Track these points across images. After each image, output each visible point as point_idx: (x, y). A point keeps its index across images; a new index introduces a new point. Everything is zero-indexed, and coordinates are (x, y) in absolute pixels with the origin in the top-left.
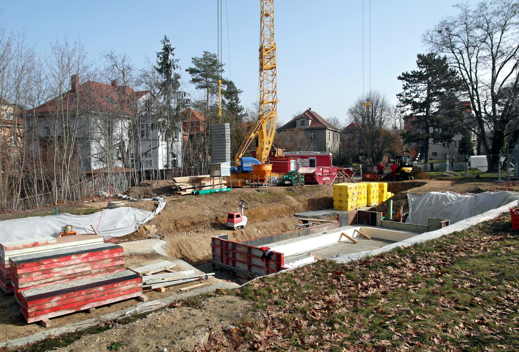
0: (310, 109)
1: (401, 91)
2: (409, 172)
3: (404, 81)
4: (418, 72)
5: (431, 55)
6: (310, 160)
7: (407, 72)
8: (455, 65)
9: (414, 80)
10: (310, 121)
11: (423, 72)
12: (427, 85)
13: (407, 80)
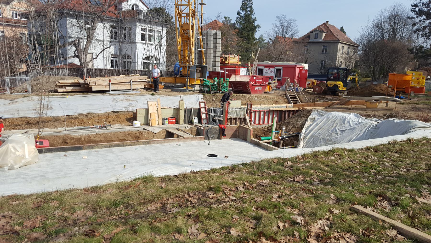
0: (327, 22)
2: (332, 86)
6: (277, 70)
10: (324, 35)
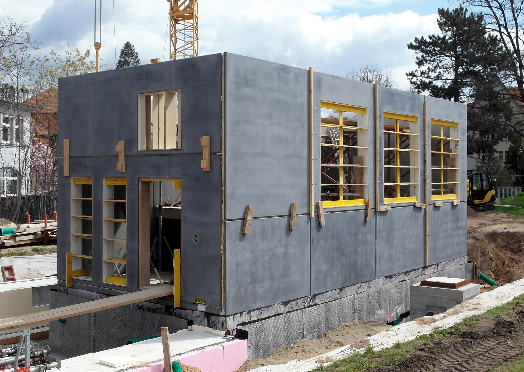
1: (414, 67)
3: (418, 51)
5: (460, 11)
7: (422, 38)
8: (492, 27)
9: (434, 50)
11: (447, 38)
12: (453, 59)
13: (422, 51)
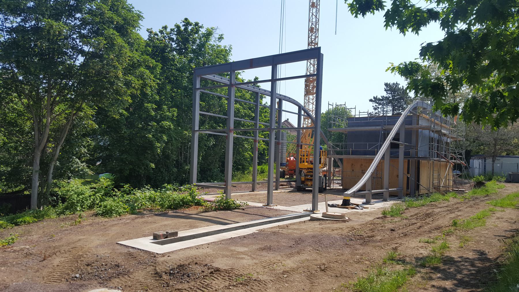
3: (374, 103)
4: (386, 97)
